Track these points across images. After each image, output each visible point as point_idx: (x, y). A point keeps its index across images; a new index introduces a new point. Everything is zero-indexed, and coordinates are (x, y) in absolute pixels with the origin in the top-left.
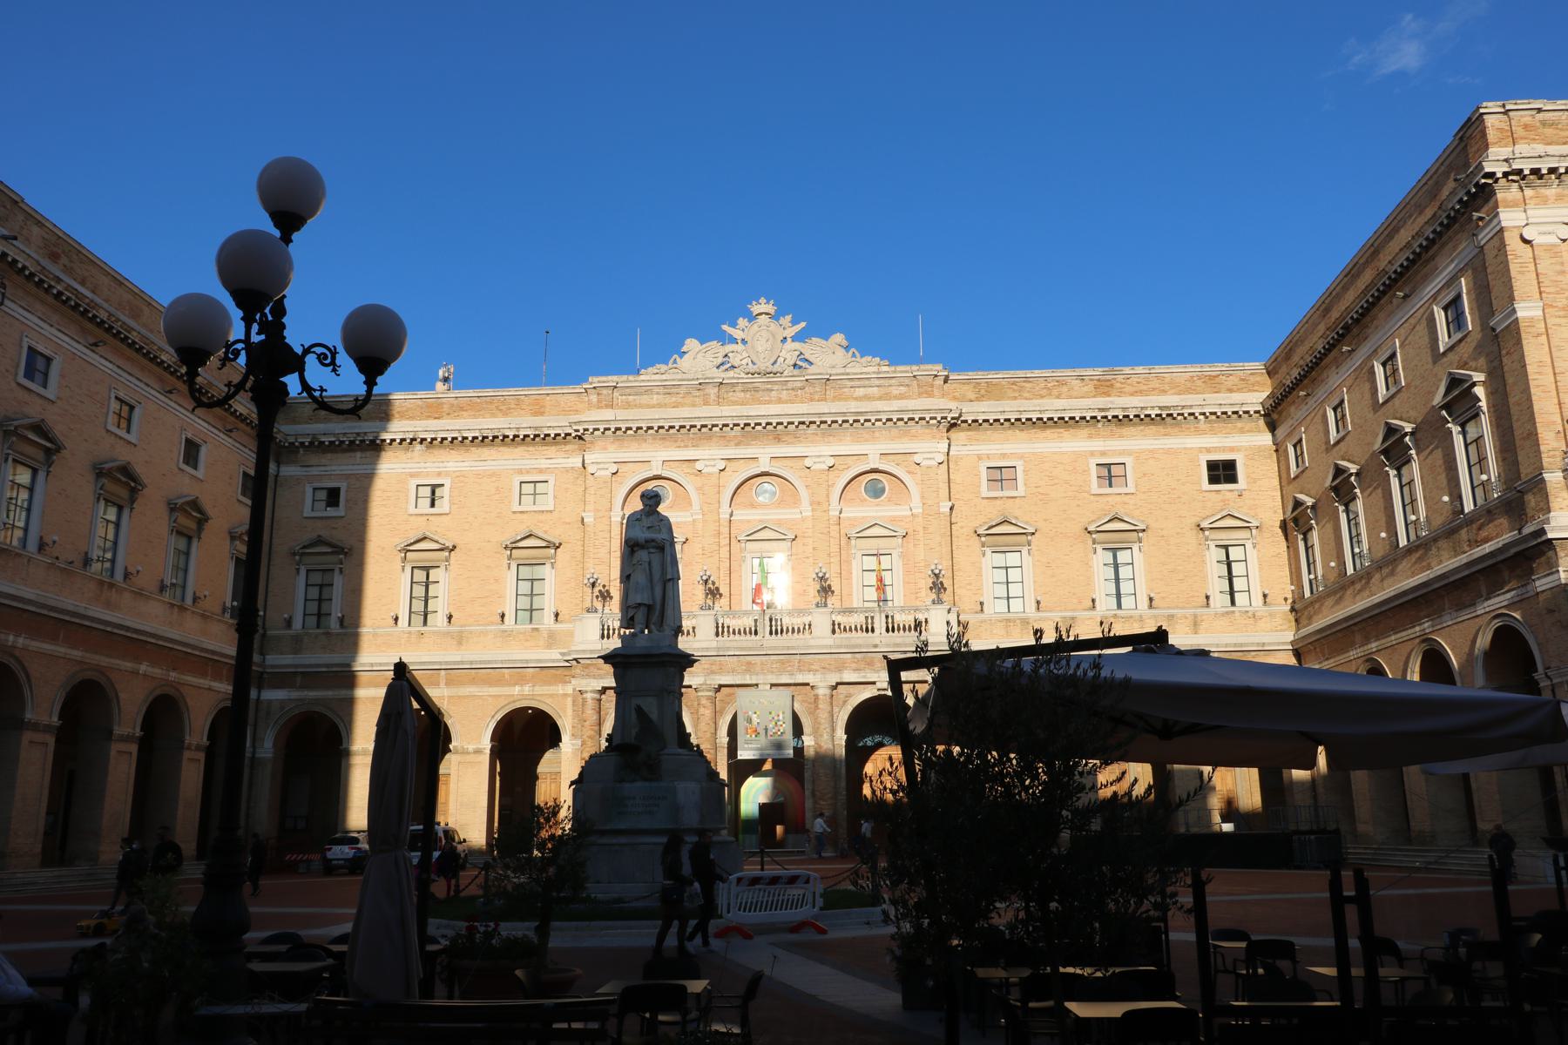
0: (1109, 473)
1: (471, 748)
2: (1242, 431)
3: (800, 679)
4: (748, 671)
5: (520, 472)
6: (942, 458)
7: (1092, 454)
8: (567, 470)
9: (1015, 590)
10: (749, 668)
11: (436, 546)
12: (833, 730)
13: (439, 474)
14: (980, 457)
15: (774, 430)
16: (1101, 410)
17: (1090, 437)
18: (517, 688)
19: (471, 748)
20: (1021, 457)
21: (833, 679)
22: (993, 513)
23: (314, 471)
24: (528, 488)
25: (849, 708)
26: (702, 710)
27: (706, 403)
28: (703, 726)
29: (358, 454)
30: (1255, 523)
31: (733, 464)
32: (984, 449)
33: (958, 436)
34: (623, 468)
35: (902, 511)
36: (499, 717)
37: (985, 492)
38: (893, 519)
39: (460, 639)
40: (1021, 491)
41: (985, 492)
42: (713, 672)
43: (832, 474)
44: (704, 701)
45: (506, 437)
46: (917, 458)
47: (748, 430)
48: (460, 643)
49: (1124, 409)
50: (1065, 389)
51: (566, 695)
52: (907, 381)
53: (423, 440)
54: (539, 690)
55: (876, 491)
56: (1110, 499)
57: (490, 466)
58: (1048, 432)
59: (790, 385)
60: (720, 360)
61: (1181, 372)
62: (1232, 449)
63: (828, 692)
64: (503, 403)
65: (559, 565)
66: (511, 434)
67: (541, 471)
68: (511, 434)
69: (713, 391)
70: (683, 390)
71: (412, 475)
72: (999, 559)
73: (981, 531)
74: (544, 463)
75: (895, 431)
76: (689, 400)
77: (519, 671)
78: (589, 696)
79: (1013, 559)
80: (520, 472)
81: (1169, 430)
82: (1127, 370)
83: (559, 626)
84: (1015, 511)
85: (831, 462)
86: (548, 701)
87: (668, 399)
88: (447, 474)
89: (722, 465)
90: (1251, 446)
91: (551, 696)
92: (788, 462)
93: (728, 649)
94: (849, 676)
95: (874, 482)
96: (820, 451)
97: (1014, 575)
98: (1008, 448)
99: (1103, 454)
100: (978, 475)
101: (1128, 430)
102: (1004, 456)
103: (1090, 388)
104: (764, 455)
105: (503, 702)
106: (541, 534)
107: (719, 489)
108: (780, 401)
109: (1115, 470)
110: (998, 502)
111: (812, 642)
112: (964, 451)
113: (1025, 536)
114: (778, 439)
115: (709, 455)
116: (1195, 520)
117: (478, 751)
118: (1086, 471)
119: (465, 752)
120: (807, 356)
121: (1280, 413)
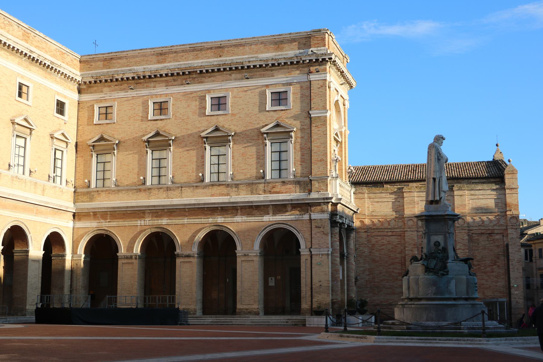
61: (54, 45)
62: (65, 97)
82: (37, 32)
90: (71, 96)
99: (23, 77)
101: (35, 68)
103: (20, 33)
116: (49, 131)
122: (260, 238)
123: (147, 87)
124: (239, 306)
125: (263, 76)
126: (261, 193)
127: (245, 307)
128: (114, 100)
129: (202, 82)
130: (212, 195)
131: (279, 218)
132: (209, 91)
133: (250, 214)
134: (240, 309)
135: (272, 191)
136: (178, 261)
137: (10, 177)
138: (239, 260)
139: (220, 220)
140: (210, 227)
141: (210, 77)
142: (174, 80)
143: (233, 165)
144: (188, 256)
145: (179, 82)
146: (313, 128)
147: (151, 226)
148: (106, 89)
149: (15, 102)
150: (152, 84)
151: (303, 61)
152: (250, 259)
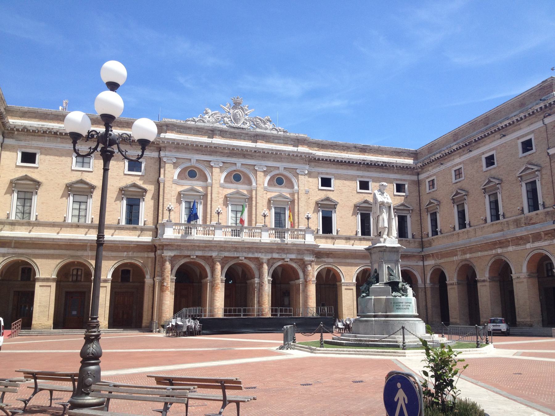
2: (408, 174)
4: (235, 251)
14: (319, 173)
17: (358, 170)
18: (125, 253)
23: (23, 143)
29: (46, 138)
30: (411, 209)
31: (226, 164)
33: (313, 164)
34: (179, 161)
51: (148, 257)
62: (404, 180)
81: (384, 171)
84: (331, 196)
92: (247, 166)
94: (276, 256)
99: (362, 177)
102: (327, 174)
104: (239, 162)
121: (423, 169)
122: (526, 263)
123: (450, 160)
124: (518, 319)
125: (514, 131)
126: (523, 225)
127: (522, 320)
128: (434, 175)
129: (479, 148)
130: (494, 232)
131: (537, 244)
132: (483, 153)
133: (518, 244)
134: (519, 322)
135: (531, 222)
136: (479, 285)
138: (514, 282)
139: (499, 251)
140: (494, 257)
141: (482, 142)
142: (464, 151)
143: (503, 206)
144: (484, 281)
145: (466, 151)
146: (552, 164)
147: (462, 261)
148: (430, 168)
150: (452, 158)
151: (537, 110)
152: (521, 280)
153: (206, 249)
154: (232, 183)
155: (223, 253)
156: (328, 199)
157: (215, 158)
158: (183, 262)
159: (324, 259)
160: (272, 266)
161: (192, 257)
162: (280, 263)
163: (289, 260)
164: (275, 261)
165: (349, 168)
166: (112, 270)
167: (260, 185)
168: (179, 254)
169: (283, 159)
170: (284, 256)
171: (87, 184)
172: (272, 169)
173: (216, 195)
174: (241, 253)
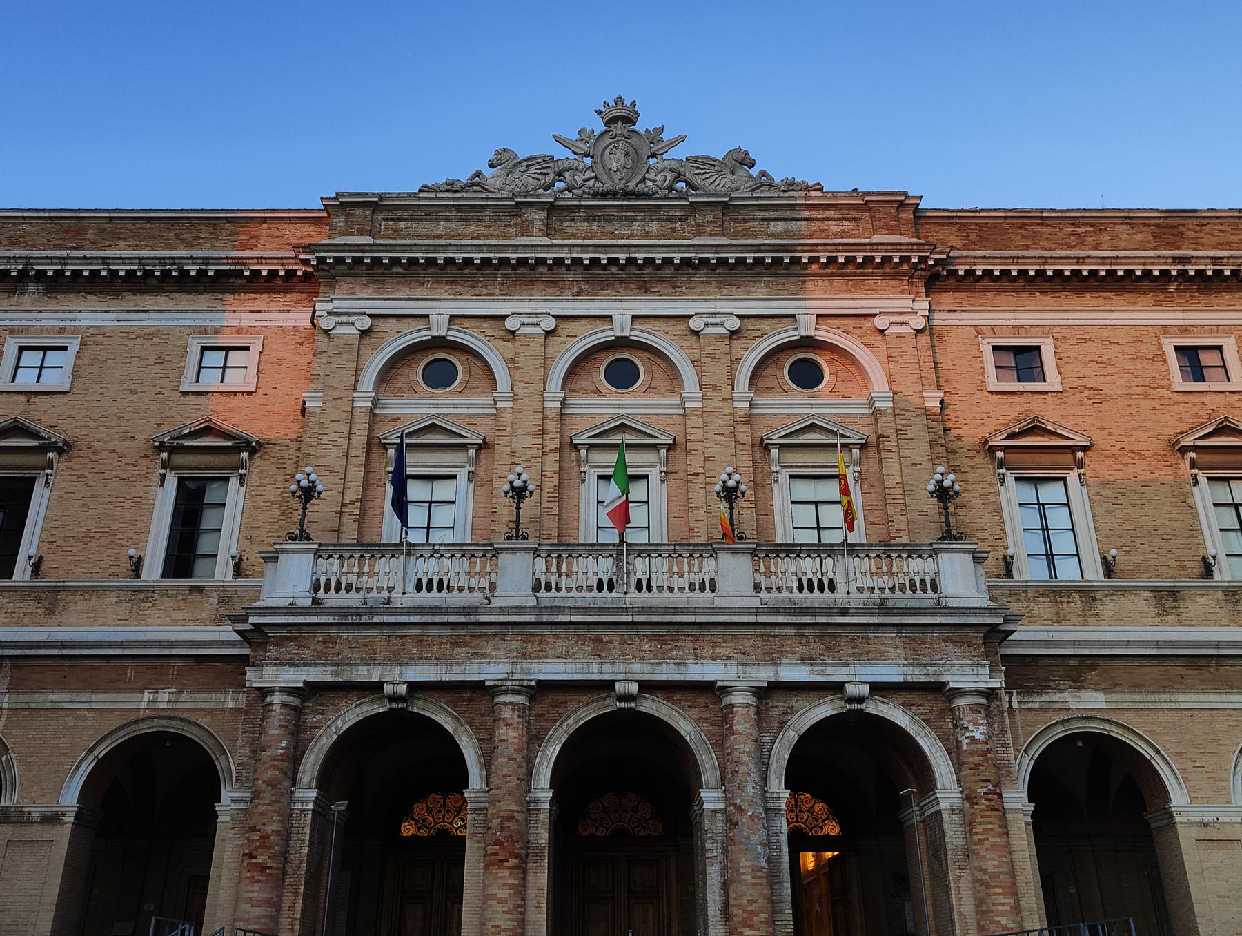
0: (1192, 360)
1: (36, 811)
3: (696, 672)
5: (204, 331)
6: (920, 323)
7: (1165, 329)
8: (284, 331)
9: (1063, 543)
10: (599, 652)
11: (35, 444)
12: (765, 779)
13: (62, 330)
14: (979, 331)
15: (641, 274)
16: (1177, 260)
17: (1158, 304)
18: (146, 696)
19: (36, 811)
20: (1046, 331)
21: (763, 674)
22: (1009, 413)
24: (215, 358)
25: (791, 737)
26: (501, 732)
27: (527, 233)
28: (503, 764)
31: (571, 326)
32: (986, 318)
33: (947, 299)
35: (855, 407)
36: (102, 751)
37: (993, 385)
38: (841, 420)
39: (50, 602)
40: (1053, 381)
41: (993, 383)
42: (526, 656)
43: (737, 345)
44: (506, 713)
45: (184, 273)
46: (880, 323)
47: (598, 274)
48: (51, 612)
49: (1215, 260)
50: (1105, 237)
52: (853, 213)
53: (41, 274)
54: (187, 700)
55: (807, 376)
56: (1206, 399)
57: (152, 320)
58: (1088, 296)
59: (663, 214)
60: (550, 178)
63: (750, 700)
64: (188, 230)
65: (253, 481)
66: (193, 269)
67: (239, 331)
68: (193, 269)
69: (538, 217)
70: (488, 215)
71: (13, 331)
72: (1028, 493)
73: (996, 441)
74: (246, 319)
75: (838, 284)
76: (497, 230)
77: (154, 665)
78: (277, 699)
79: (1050, 493)
80: (204, 331)
83: (241, 583)
85: (734, 324)
86: (204, 721)
87: (463, 228)
88: (75, 331)
89: (551, 324)
91: (211, 711)
93: (560, 610)
94: (793, 672)
95: (804, 364)
96: (716, 308)
97: (1058, 518)
98: (1025, 318)
99: (1184, 330)
100: (979, 357)
102: (1018, 329)
103: (1145, 236)
104: (622, 312)
105: (116, 721)
106: (226, 426)
107: (546, 362)
108: (647, 235)
109: (1206, 358)
110: (1016, 399)
111: (719, 603)
112: (953, 319)
113: (1074, 455)
114: (645, 289)
115: (529, 309)
117: (51, 820)
118: (1162, 355)
119: (22, 819)
120: (689, 175)
137: (1220, 595)
149: (1176, 397)
153: (458, 650)
154: (600, 394)
155: (535, 668)
156: (1036, 429)
157: (526, 304)
158: (352, 714)
159: (1056, 697)
160: (782, 724)
161: (388, 689)
162: (824, 709)
163: (865, 690)
164: (796, 702)
165: (1116, 299)
166: (86, 768)
167: (715, 387)
168: (329, 678)
169: (809, 285)
170: (836, 674)
171: (35, 435)
172: (765, 325)
173: (530, 441)
174: (622, 668)
